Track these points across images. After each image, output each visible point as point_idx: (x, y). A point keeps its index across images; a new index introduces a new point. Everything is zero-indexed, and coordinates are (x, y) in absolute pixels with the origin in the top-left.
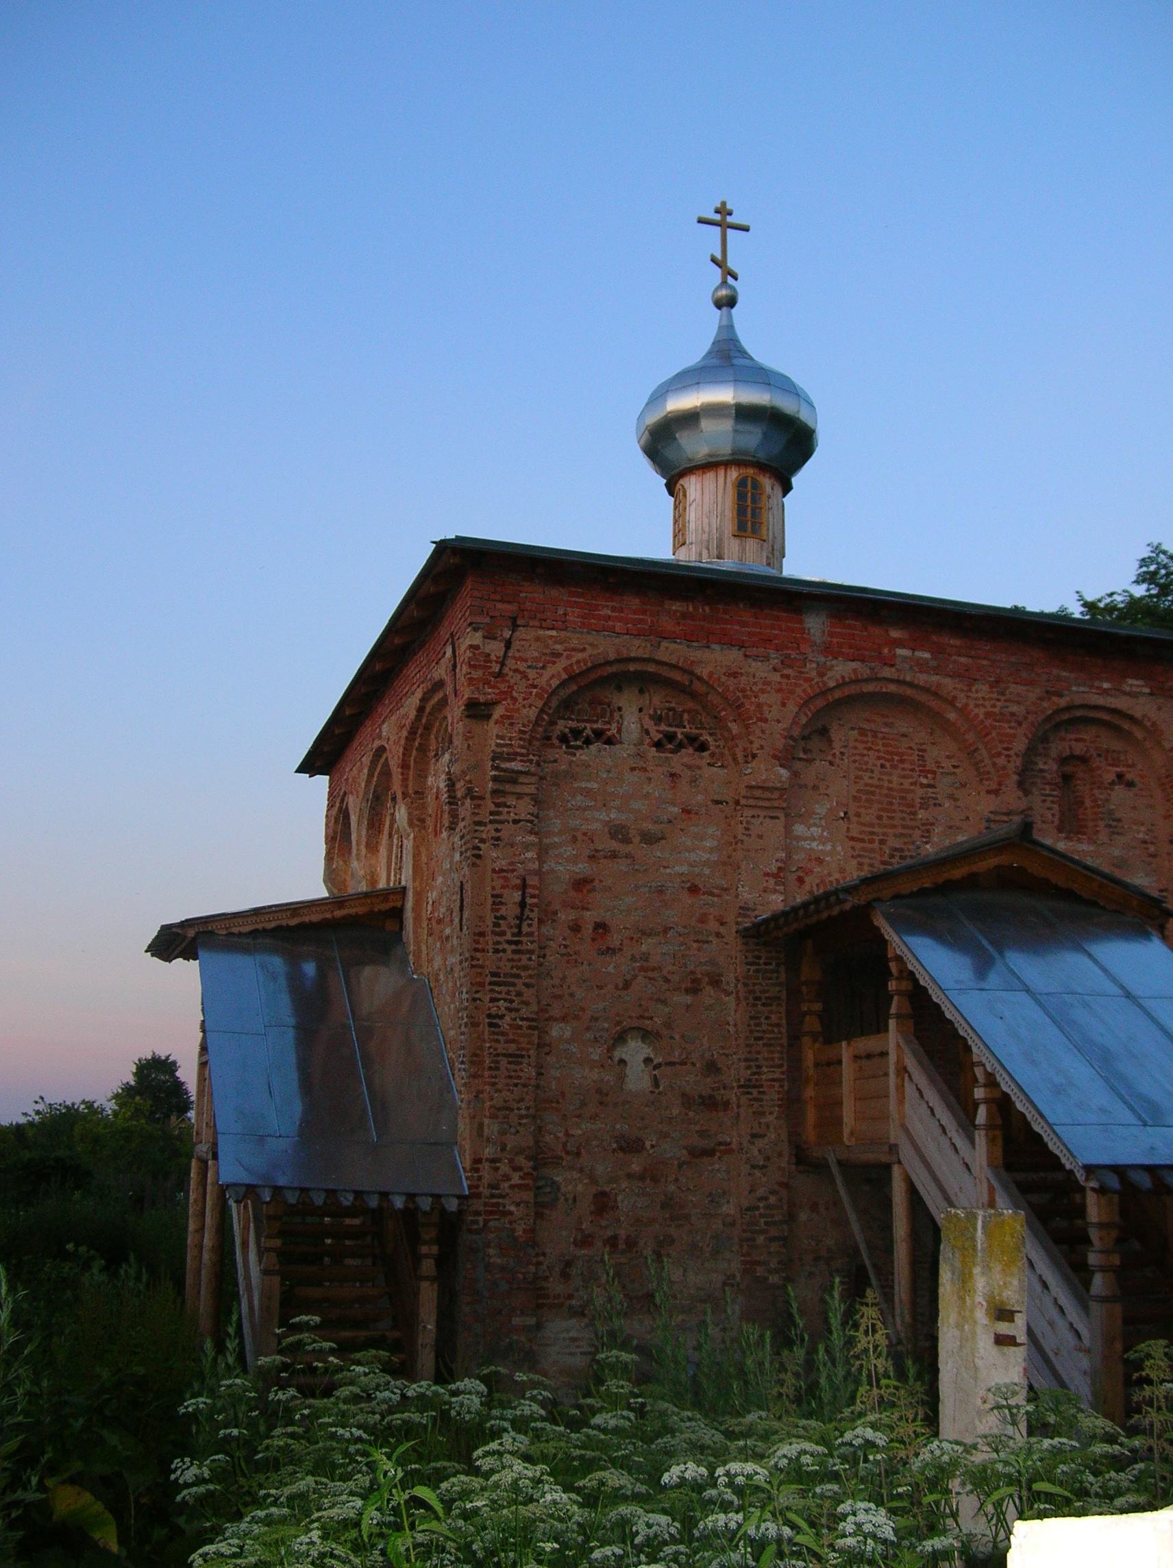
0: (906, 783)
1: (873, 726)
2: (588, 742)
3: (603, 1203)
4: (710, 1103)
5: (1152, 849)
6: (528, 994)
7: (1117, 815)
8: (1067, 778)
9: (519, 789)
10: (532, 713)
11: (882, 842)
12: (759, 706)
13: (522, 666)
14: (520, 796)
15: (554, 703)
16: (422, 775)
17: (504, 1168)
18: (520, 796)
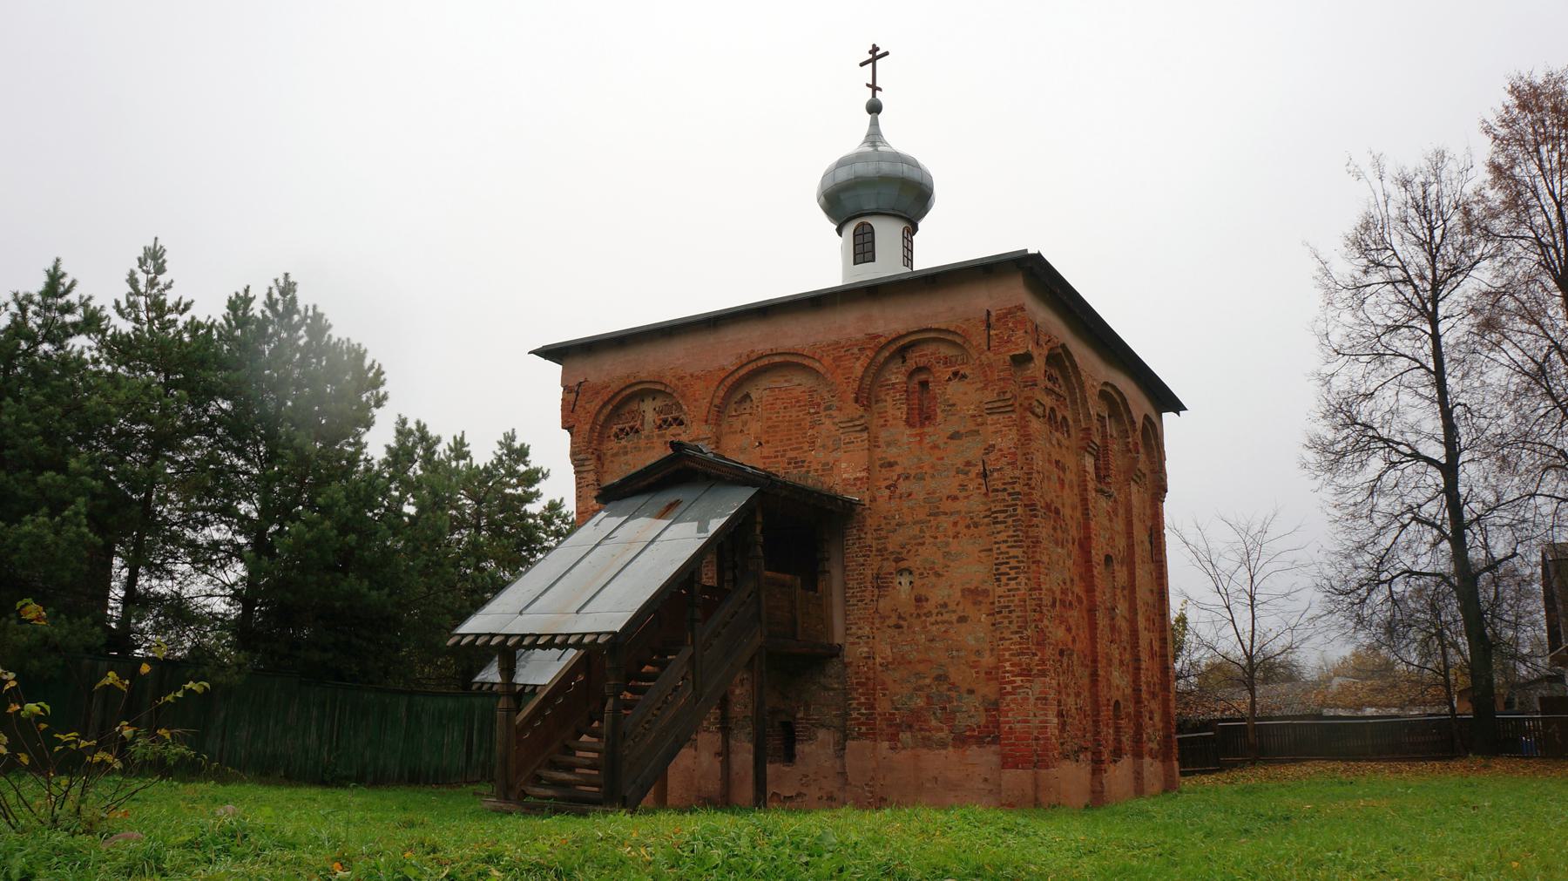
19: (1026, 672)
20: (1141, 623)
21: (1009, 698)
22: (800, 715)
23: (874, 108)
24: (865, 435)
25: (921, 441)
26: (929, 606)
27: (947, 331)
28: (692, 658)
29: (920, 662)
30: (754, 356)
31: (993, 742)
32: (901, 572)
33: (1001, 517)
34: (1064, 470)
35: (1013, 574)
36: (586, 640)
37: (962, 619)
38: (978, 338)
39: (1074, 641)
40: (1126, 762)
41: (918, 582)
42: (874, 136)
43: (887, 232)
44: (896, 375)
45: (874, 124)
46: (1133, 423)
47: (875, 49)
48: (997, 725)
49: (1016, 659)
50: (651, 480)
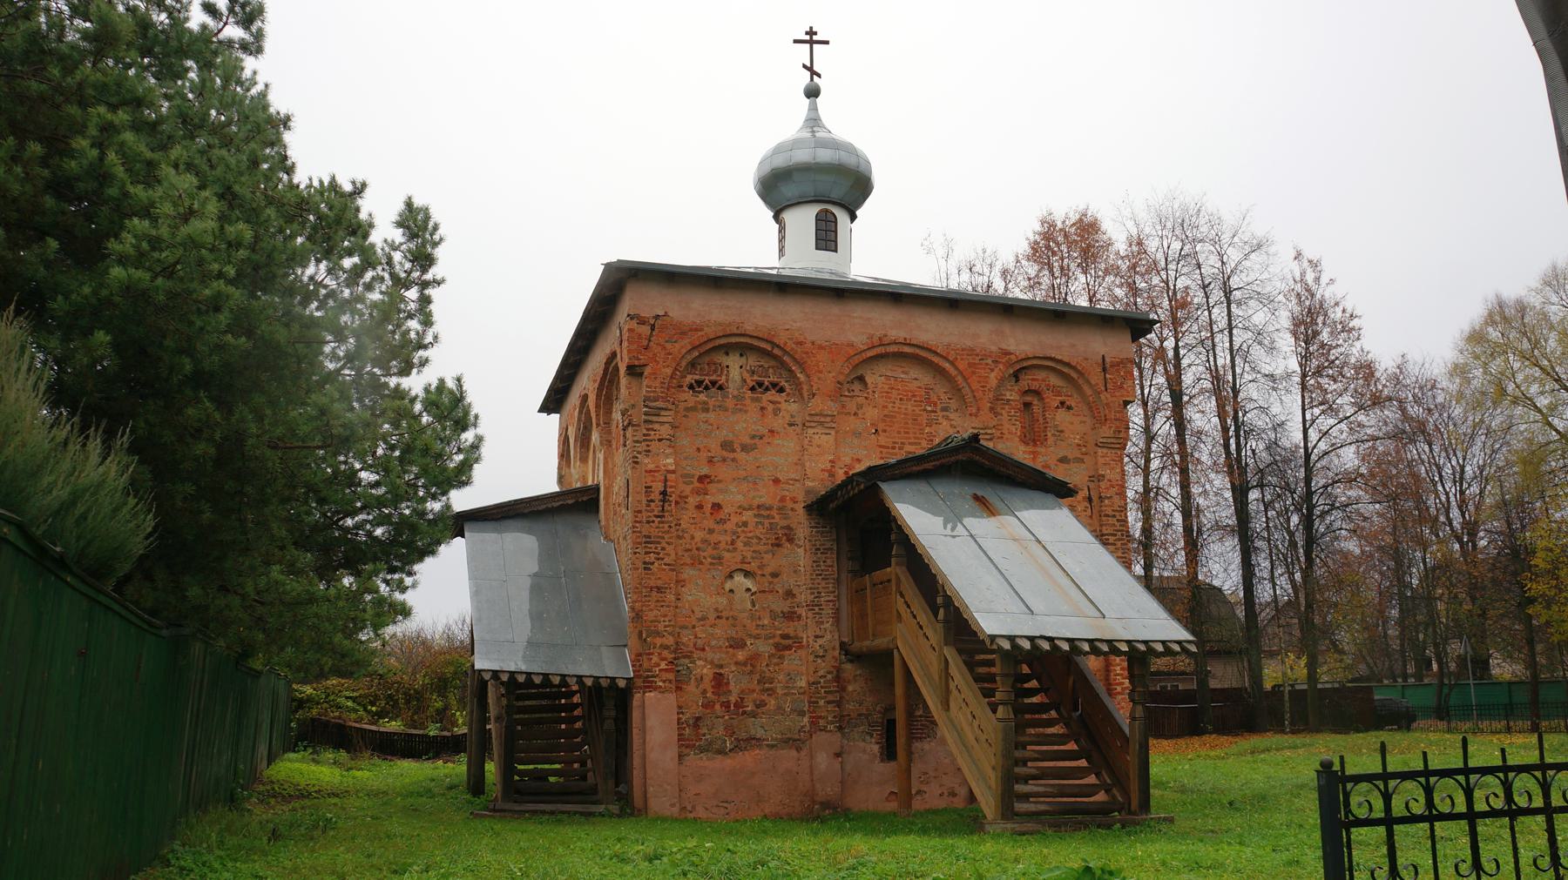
3: (719, 681)
4: (790, 616)
6: (670, 549)
8: (1027, 405)
10: (669, 371)
13: (662, 341)
15: (684, 364)
16: (609, 412)
17: (655, 659)
23: (812, 93)
27: (1068, 365)
42: (813, 121)
45: (814, 108)
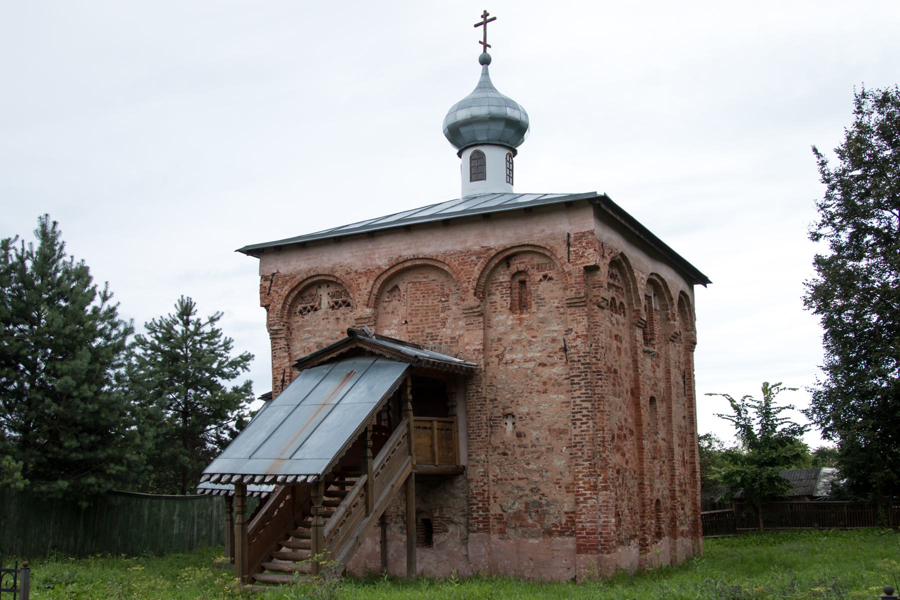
0: (435, 302)
1: (418, 280)
2: (309, 311)
5: (562, 310)
7: (542, 297)
9: (280, 336)
10: (280, 306)
11: (423, 331)
12: (358, 284)
14: (281, 338)
18: (281, 338)
19: (594, 488)
20: (676, 441)
21: (582, 505)
22: (436, 515)
23: (485, 61)
24: (481, 319)
25: (520, 324)
26: (525, 441)
27: (540, 247)
28: (366, 486)
29: (519, 479)
30: (401, 260)
31: (571, 535)
32: (506, 416)
33: (576, 380)
34: (621, 342)
35: (584, 420)
36: (300, 479)
37: (550, 450)
38: (562, 252)
39: (627, 462)
40: (666, 538)
41: (518, 424)
42: (485, 84)
43: (494, 157)
44: (503, 277)
45: (486, 73)
46: (672, 299)
47: (486, 15)
48: (573, 522)
49: (586, 479)
50: (334, 355)
